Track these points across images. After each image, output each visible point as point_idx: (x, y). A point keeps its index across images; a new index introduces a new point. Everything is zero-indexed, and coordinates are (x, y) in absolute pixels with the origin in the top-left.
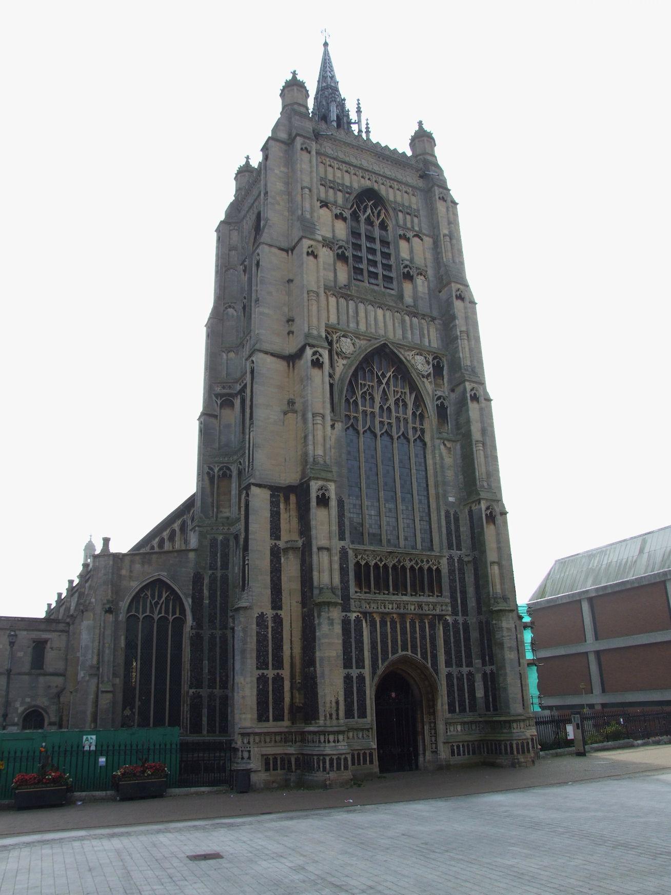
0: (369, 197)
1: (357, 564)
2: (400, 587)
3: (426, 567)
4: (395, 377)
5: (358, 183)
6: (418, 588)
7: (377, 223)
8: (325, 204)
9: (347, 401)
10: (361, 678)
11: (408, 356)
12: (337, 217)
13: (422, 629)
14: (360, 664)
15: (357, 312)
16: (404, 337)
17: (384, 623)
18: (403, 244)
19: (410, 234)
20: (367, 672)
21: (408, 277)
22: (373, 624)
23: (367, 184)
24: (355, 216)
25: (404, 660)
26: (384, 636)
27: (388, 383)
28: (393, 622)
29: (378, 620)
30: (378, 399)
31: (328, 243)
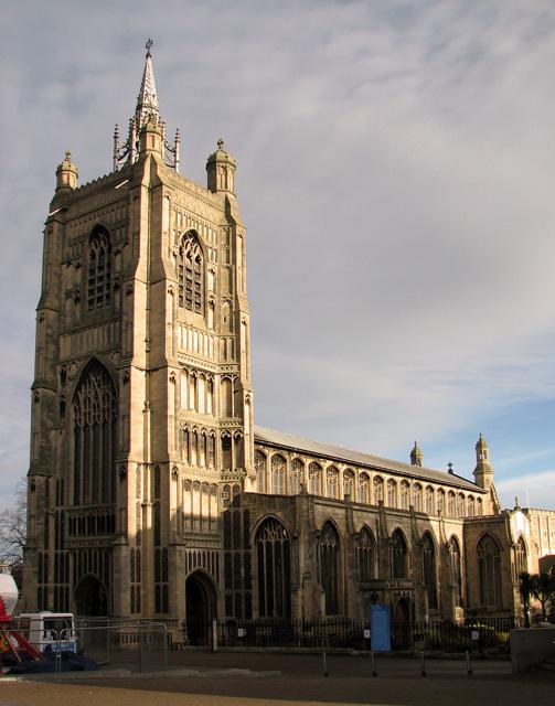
0: (99, 232)
1: (70, 520)
2: (92, 531)
3: (106, 514)
4: (103, 378)
5: (86, 227)
6: (101, 530)
7: (105, 249)
8: (69, 264)
9: (75, 410)
10: (67, 589)
11: (103, 360)
12: (78, 267)
13: (101, 557)
14: (67, 581)
15: (81, 342)
16: (109, 343)
17: (80, 555)
18: (119, 257)
19: (120, 247)
20: (71, 584)
21: (117, 287)
22: (75, 555)
23: (97, 220)
24: (93, 256)
25: (89, 576)
26: (80, 563)
27: (99, 386)
28: (85, 554)
29: (77, 551)
30: (93, 401)
31: (68, 295)
